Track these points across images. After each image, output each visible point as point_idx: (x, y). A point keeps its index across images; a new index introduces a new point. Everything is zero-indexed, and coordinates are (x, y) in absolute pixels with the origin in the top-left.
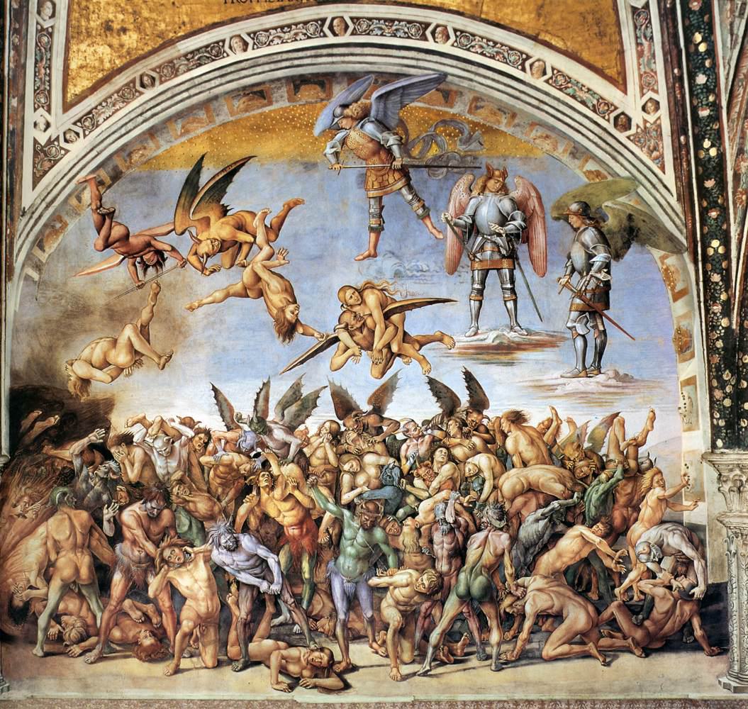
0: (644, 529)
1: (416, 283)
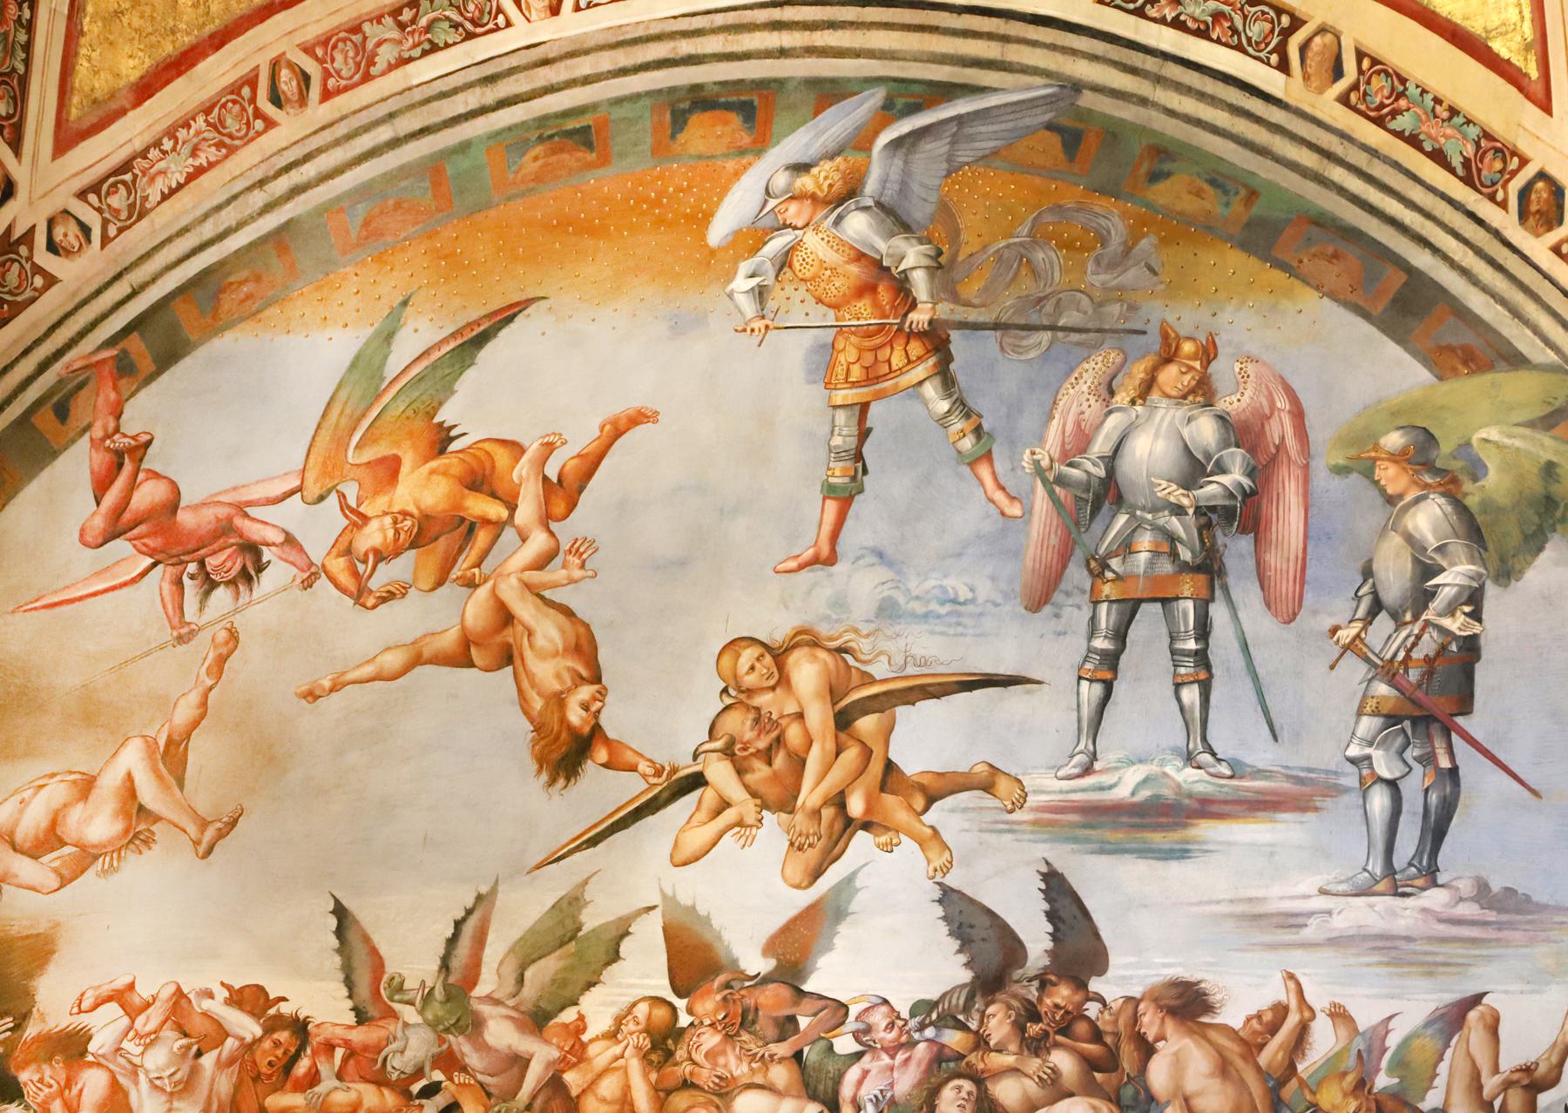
1: (932, 633)
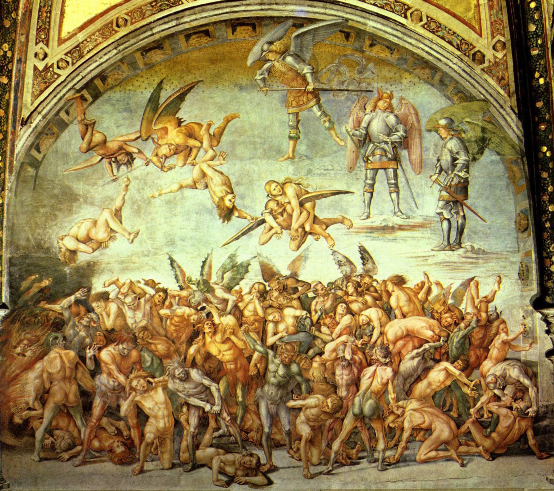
0: (492, 364)
